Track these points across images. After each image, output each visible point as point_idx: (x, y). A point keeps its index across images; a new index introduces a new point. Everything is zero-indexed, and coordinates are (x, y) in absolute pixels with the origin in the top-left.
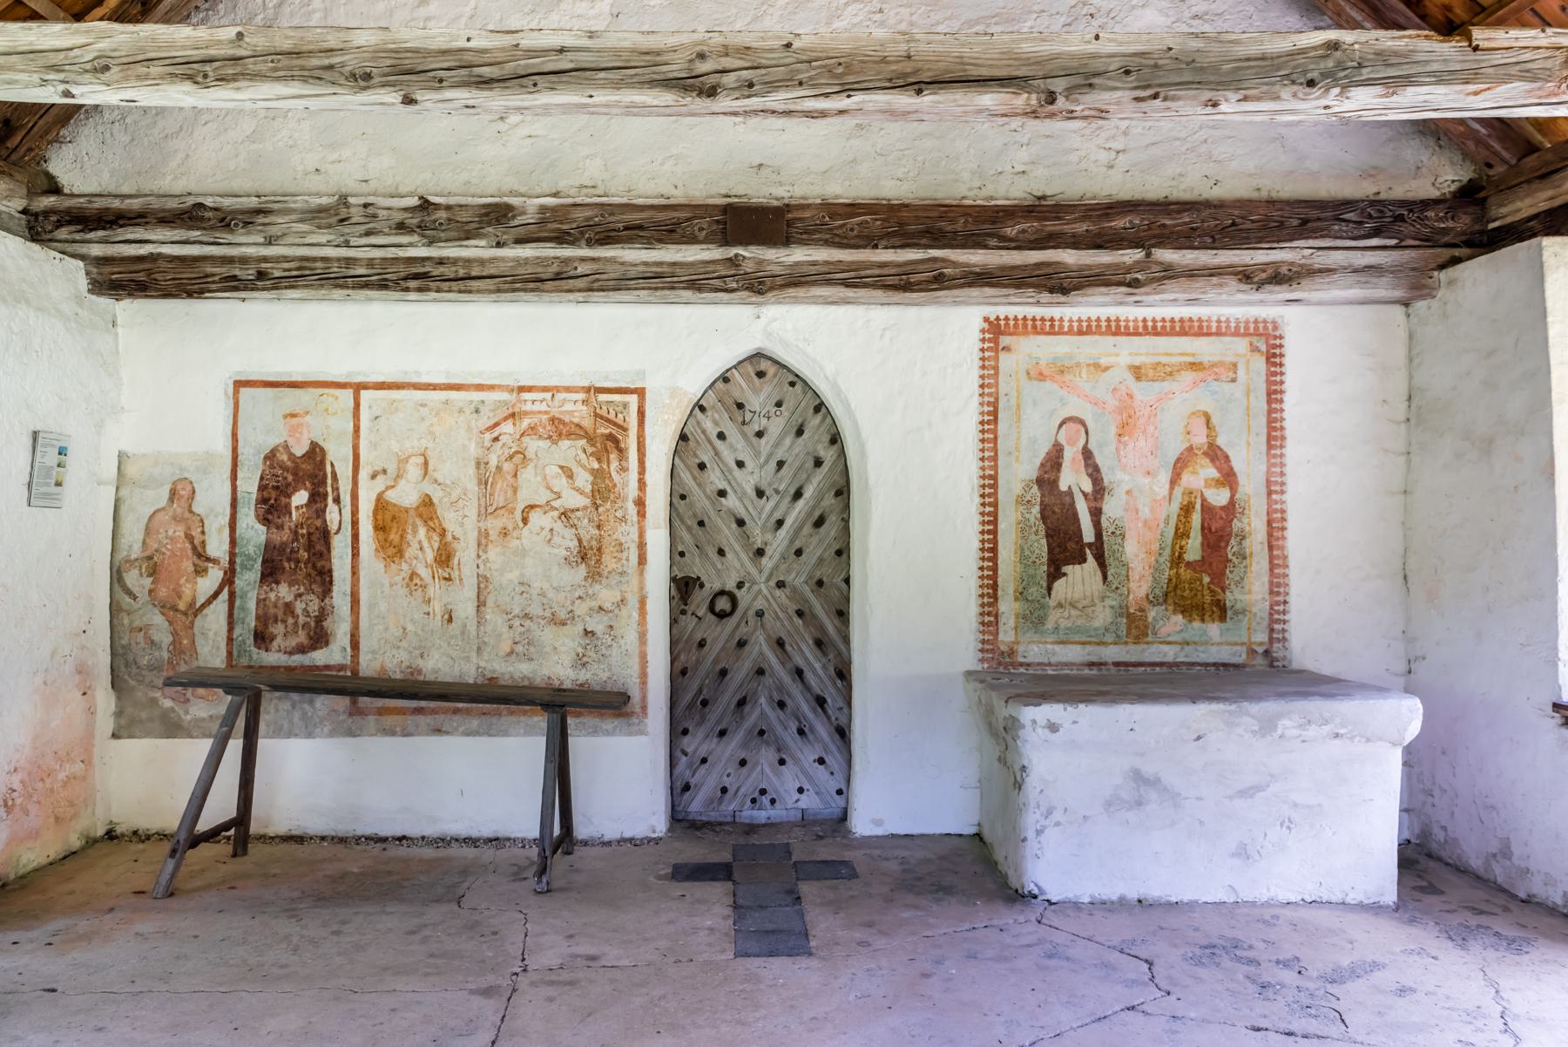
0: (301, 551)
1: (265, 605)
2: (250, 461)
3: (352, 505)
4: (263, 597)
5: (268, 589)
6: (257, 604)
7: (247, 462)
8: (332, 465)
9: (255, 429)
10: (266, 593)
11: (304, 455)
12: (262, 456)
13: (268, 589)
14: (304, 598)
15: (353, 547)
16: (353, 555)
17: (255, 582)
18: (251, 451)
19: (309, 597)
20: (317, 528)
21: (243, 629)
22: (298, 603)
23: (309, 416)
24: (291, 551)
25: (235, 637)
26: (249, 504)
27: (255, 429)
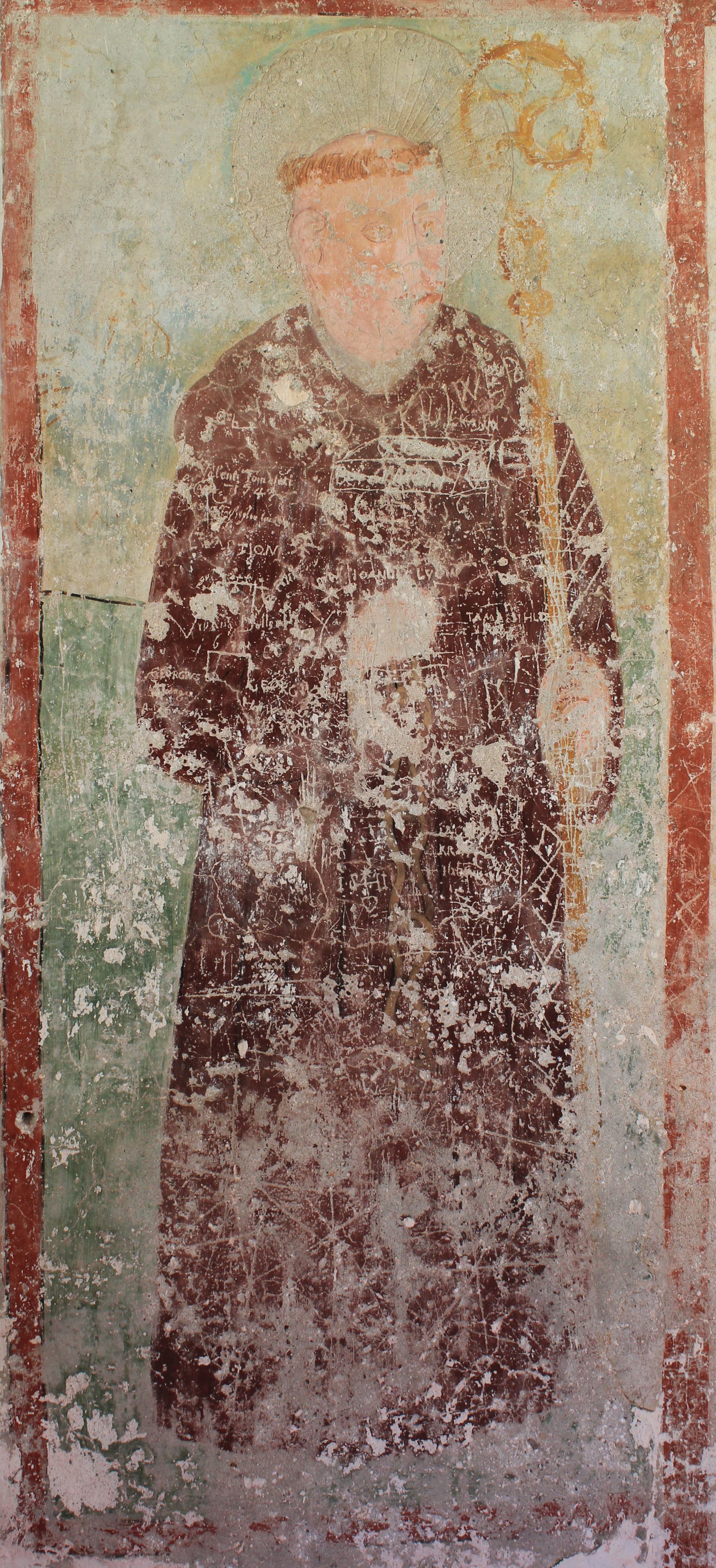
0: (400, 915)
1: (214, 1211)
2: (107, 423)
3: (679, 655)
4: (197, 1166)
5: (224, 1125)
6: (167, 1207)
7: (91, 432)
8: (561, 434)
9: (129, 246)
10: (212, 1143)
11: (405, 389)
12: (178, 397)
13: (224, 1125)
14: (417, 1163)
15: (675, 885)
16: (674, 929)
17: (146, 1086)
18: (115, 366)
19: (444, 1159)
20: (488, 791)
21: (95, 1337)
22: (388, 1190)
23: (428, 171)
24: (343, 918)
25: (49, 1374)
26: (106, 659)
27: (129, 246)
